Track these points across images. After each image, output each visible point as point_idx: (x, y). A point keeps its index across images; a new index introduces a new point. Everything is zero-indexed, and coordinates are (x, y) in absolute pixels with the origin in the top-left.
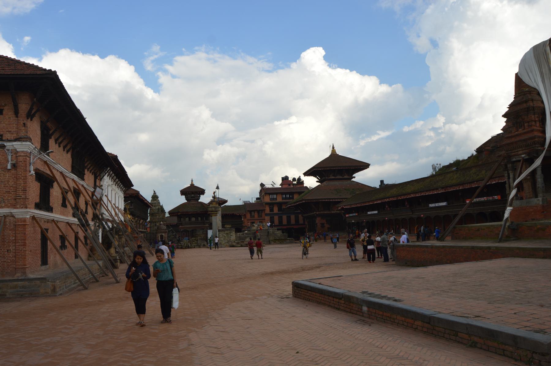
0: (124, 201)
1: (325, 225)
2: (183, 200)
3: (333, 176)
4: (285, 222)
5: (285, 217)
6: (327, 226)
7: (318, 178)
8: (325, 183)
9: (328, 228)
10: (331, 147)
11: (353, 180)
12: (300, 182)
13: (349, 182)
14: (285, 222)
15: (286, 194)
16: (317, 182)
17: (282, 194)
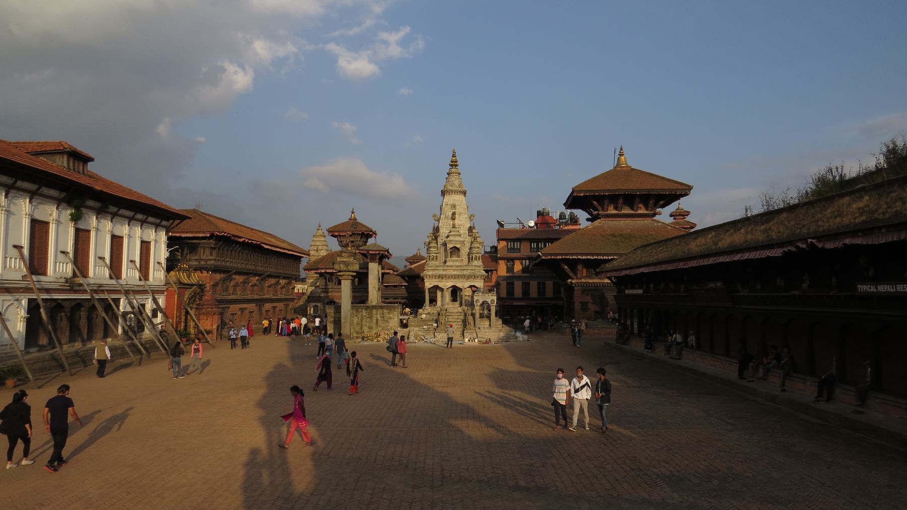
0: (169, 246)
1: (590, 305)
2: (334, 245)
3: (616, 208)
4: (534, 293)
5: (534, 285)
6: (593, 308)
7: (590, 214)
8: (597, 223)
9: (596, 312)
10: (617, 153)
11: (657, 218)
12: (574, 220)
13: (647, 221)
14: (534, 293)
15: (537, 241)
16: (588, 220)
17: (531, 241)
